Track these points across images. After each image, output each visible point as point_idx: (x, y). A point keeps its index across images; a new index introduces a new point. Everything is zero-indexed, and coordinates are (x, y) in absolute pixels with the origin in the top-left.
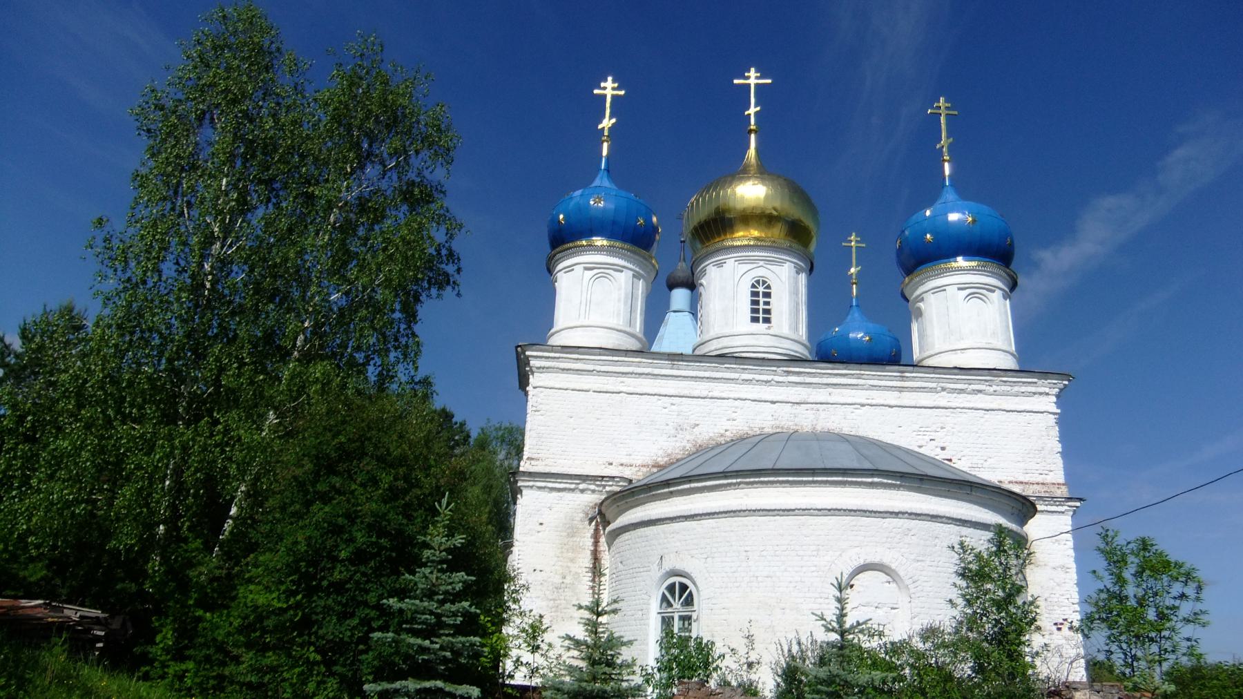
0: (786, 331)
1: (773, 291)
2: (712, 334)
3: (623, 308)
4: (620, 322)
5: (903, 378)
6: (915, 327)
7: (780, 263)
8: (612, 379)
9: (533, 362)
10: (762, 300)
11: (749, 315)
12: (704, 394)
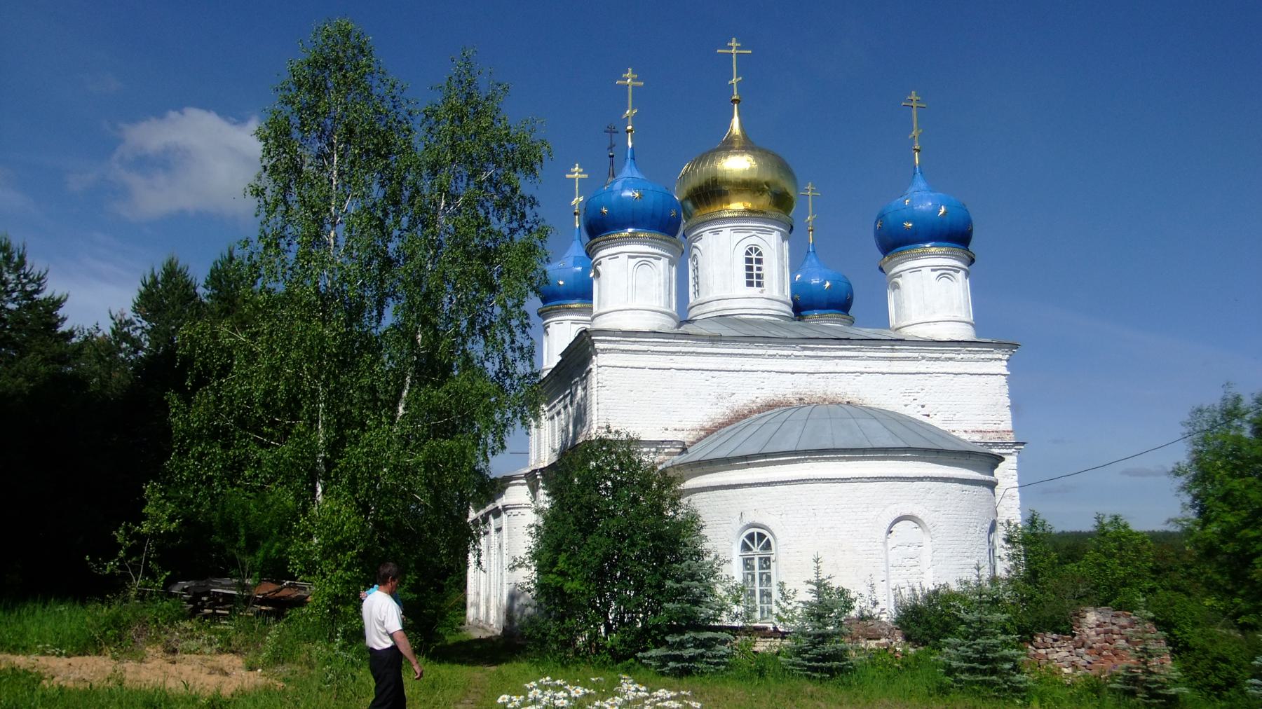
0: (776, 293)
1: (764, 257)
2: (712, 296)
3: (662, 291)
4: (660, 304)
5: (893, 350)
6: (891, 296)
7: (770, 232)
8: (663, 358)
9: (597, 345)
10: (755, 266)
11: (744, 280)
12: (738, 368)
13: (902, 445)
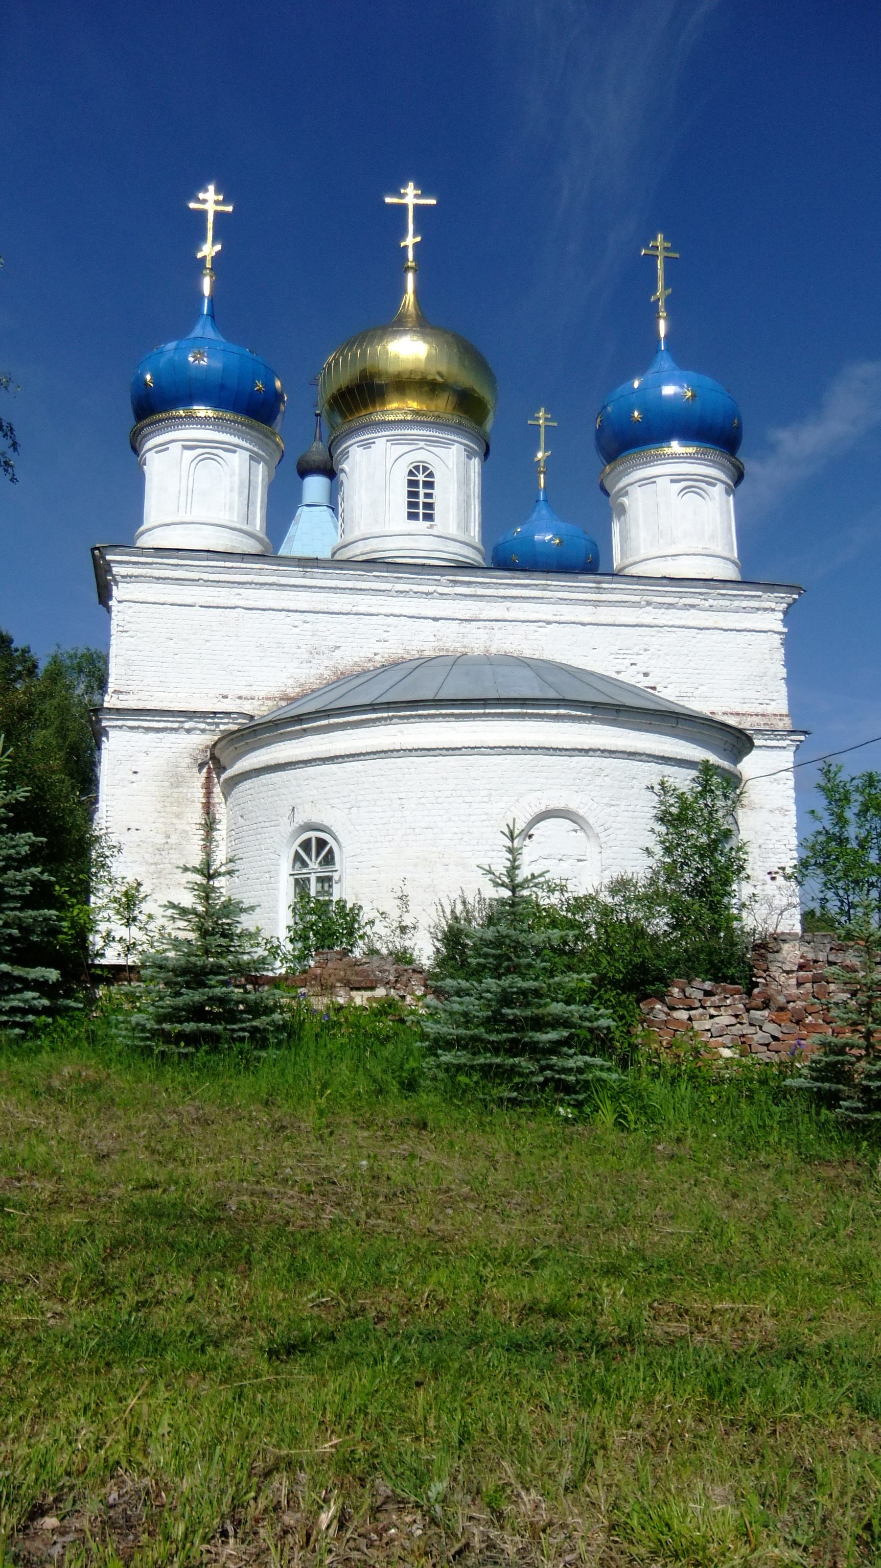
0: (453, 530)
1: (437, 480)
2: (357, 534)
3: (236, 500)
4: (234, 517)
5: (599, 590)
6: (616, 527)
7: (447, 444)
9: (116, 570)
10: (422, 491)
11: (405, 510)
12: (347, 608)
13: (552, 695)
